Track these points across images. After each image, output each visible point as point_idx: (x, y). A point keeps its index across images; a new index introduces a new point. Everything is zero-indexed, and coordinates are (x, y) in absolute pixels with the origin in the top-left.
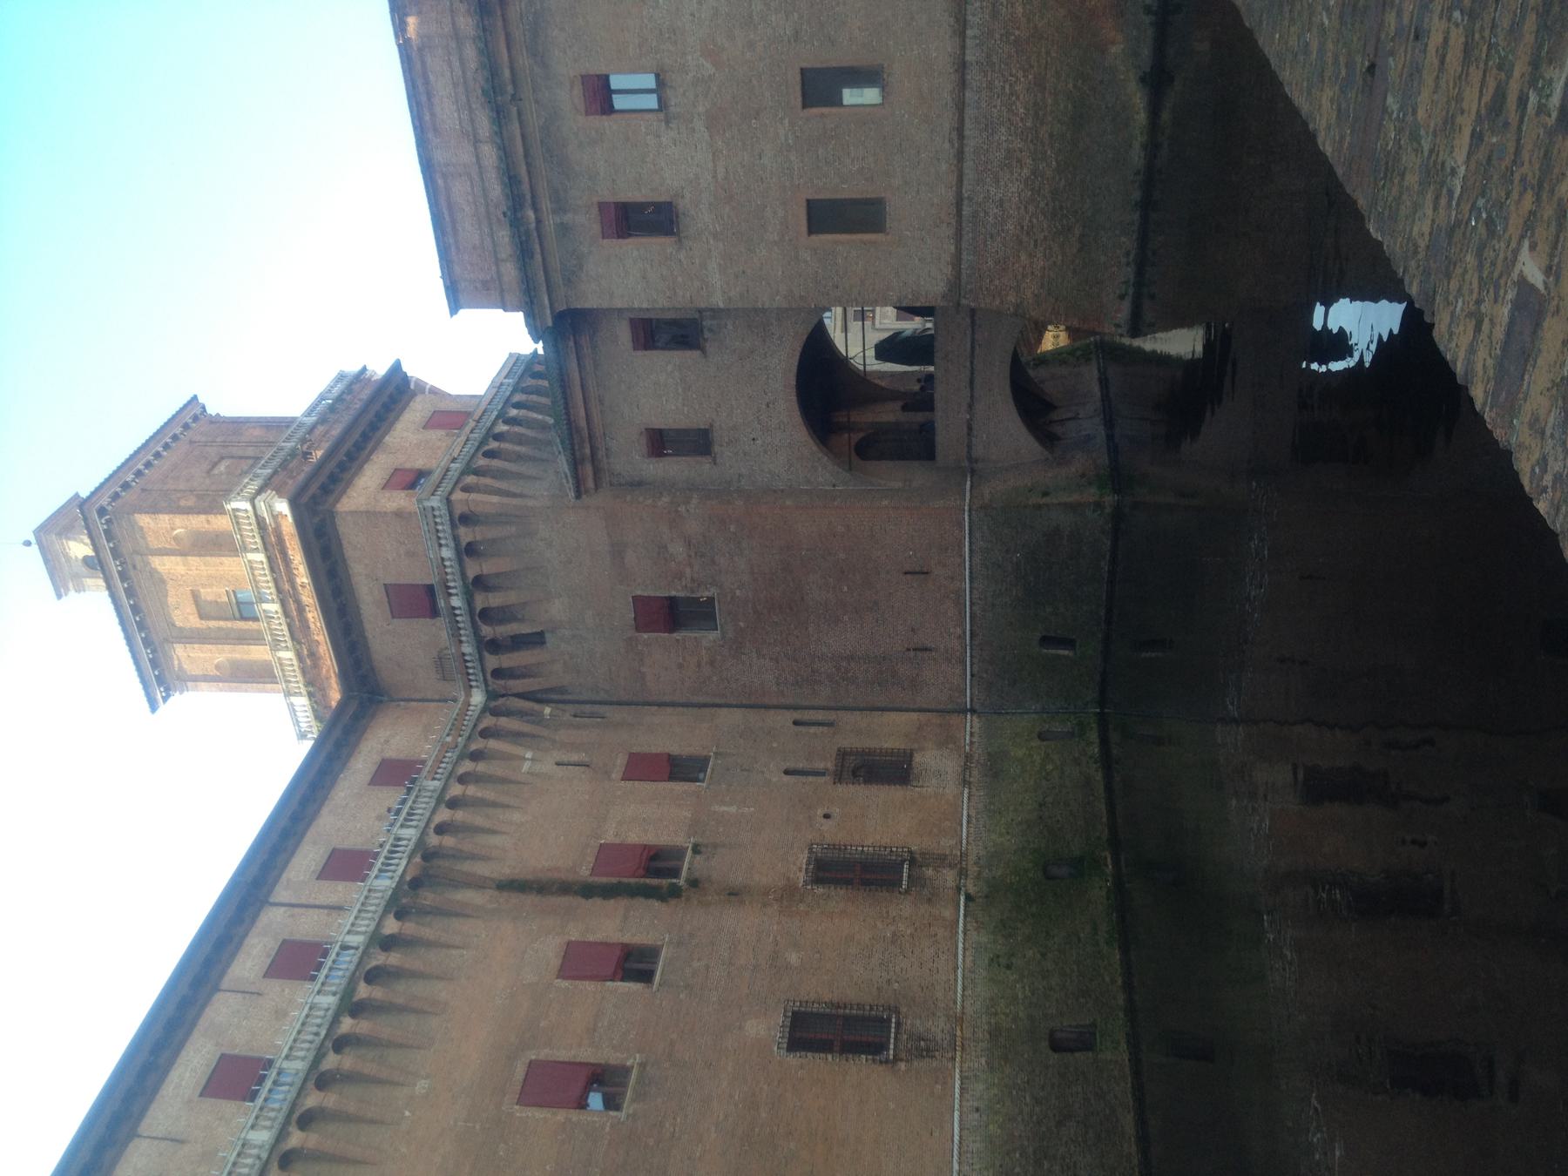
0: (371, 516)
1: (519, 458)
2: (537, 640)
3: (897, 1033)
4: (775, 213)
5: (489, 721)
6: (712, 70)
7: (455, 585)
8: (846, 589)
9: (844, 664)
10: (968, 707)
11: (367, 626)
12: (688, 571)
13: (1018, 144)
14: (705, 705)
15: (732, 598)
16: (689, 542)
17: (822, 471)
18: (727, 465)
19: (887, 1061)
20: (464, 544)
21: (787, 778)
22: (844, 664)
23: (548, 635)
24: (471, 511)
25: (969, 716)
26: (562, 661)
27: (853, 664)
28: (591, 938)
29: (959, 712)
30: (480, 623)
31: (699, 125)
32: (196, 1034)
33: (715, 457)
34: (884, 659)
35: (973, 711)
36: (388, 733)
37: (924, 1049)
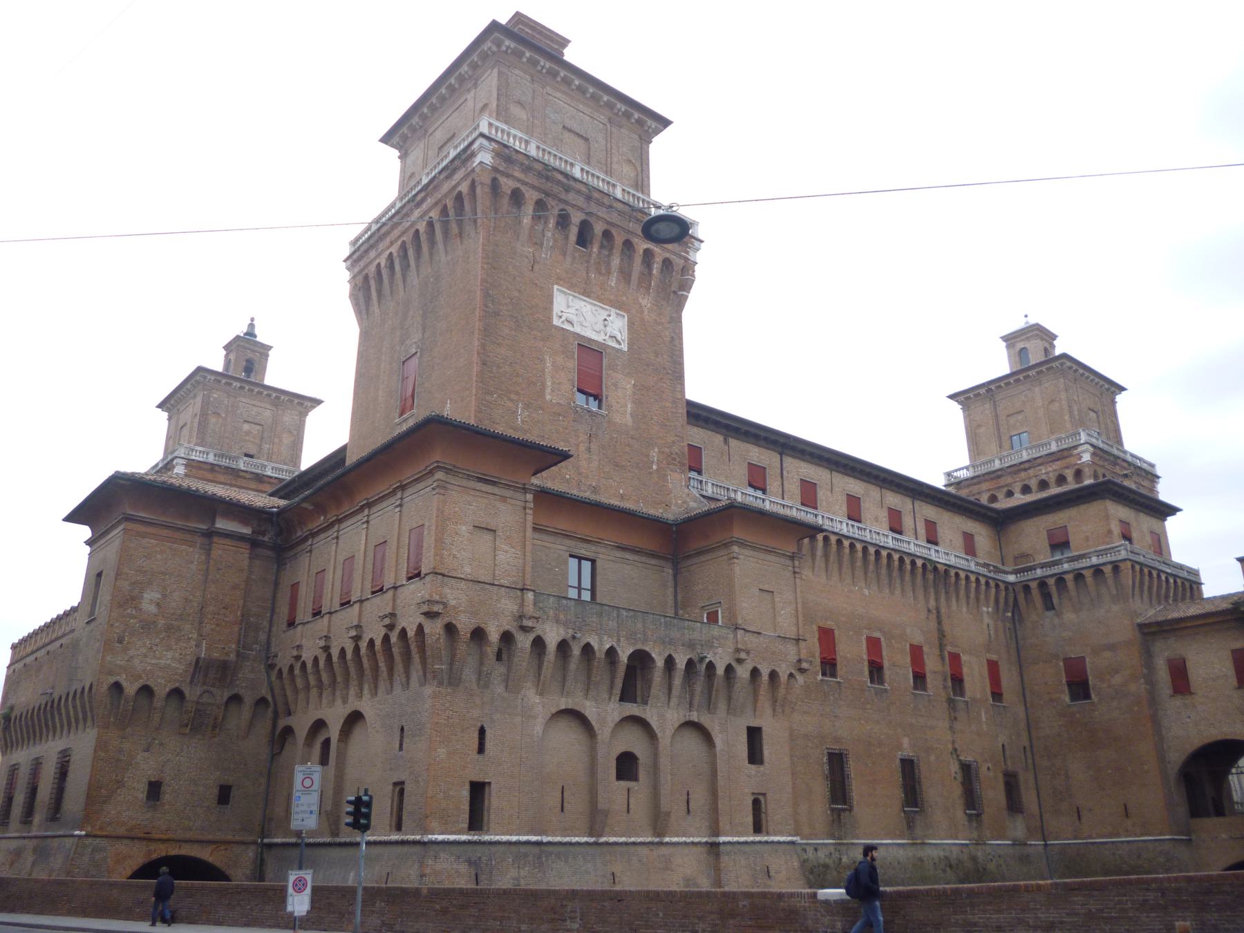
1: (1150, 588)
5: (1002, 586)
7: (1077, 565)
8: (1109, 771)
10: (1048, 842)
17: (1176, 758)
19: (903, 807)
20: (1102, 568)
21: (1000, 745)
23: (1053, 612)
25: (1043, 843)
28: (925, 657)
32: (865, 484)
35: (1046, 845)
36: (984, 534)
37: (910, 825)
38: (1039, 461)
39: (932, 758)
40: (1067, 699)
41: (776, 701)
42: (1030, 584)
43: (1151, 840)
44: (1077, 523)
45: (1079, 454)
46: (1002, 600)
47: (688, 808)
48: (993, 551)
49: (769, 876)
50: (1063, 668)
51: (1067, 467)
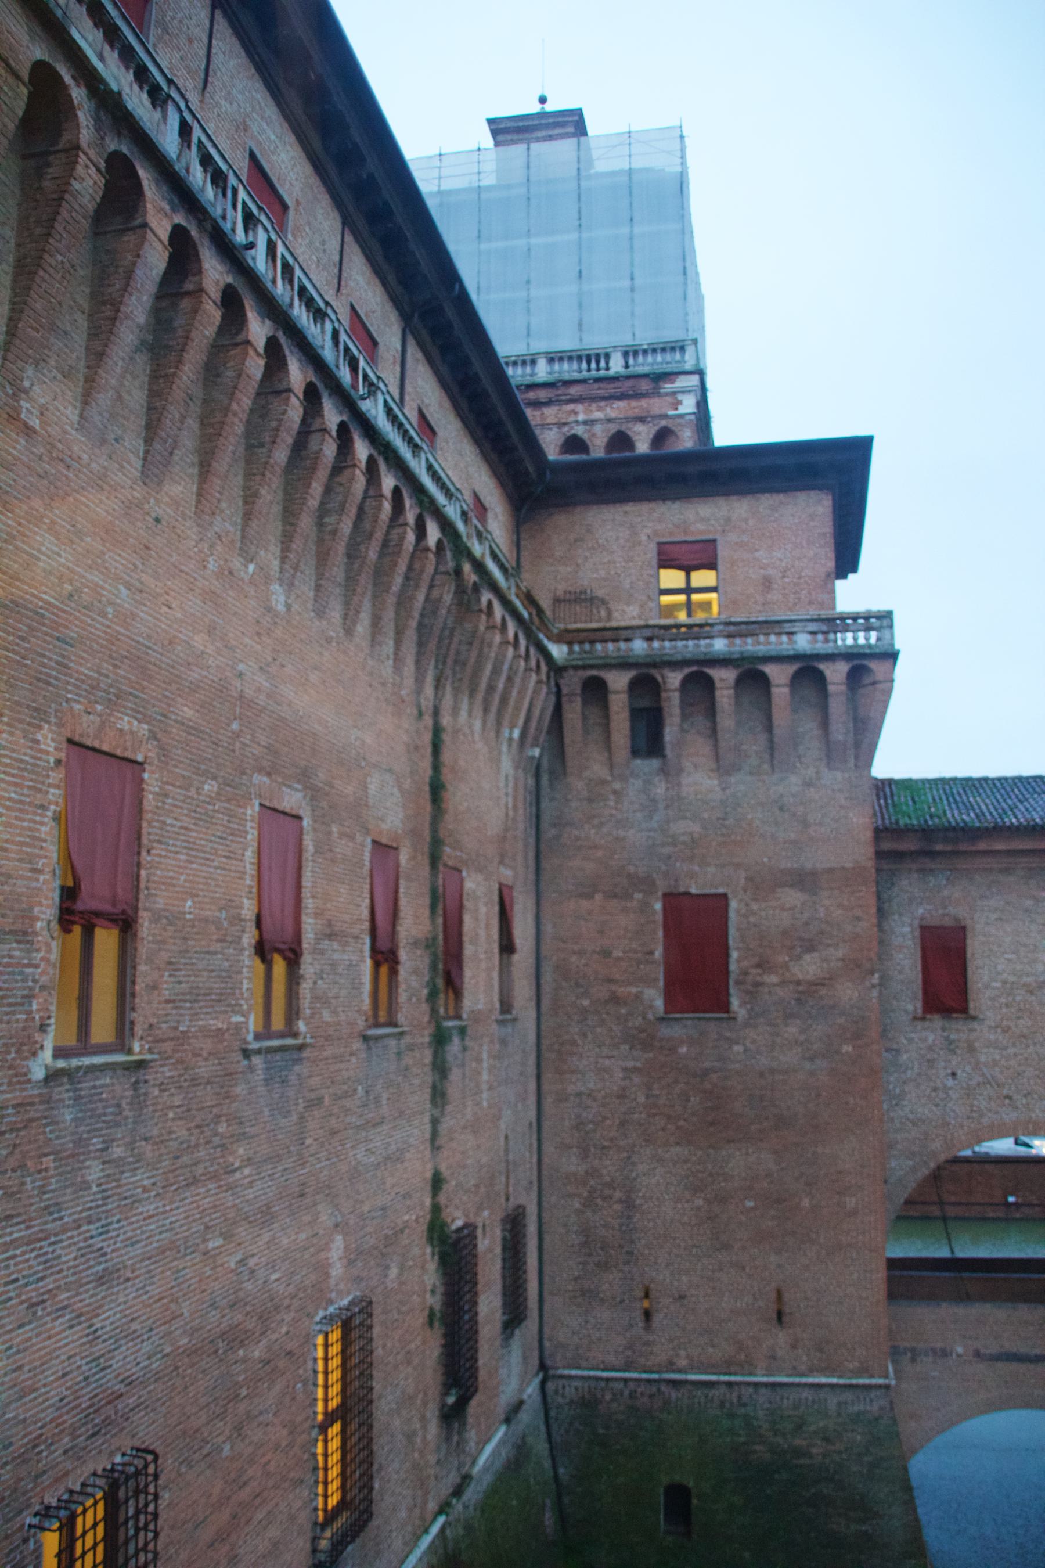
7: (750, 646)
8: (750, 1204)
11: (645, 507)
12: (774, 979)
15: (728, 1038)
16: (823, 985)
18: (913, 1035)
20: (822, 666)
22: (618, 1194)
23: (655, 763)
24: (874, 683)
26: (609, 778)
27: (617, 1207)
30: (687, 671)
33: (923, 1019)
34: (630, 1253)
38: (574, 390)
40: (659, 1003)
43: (832, 1386)
44: (745, 538)
45: (674, 394)
50: (659, 917)
51: (641, 420)
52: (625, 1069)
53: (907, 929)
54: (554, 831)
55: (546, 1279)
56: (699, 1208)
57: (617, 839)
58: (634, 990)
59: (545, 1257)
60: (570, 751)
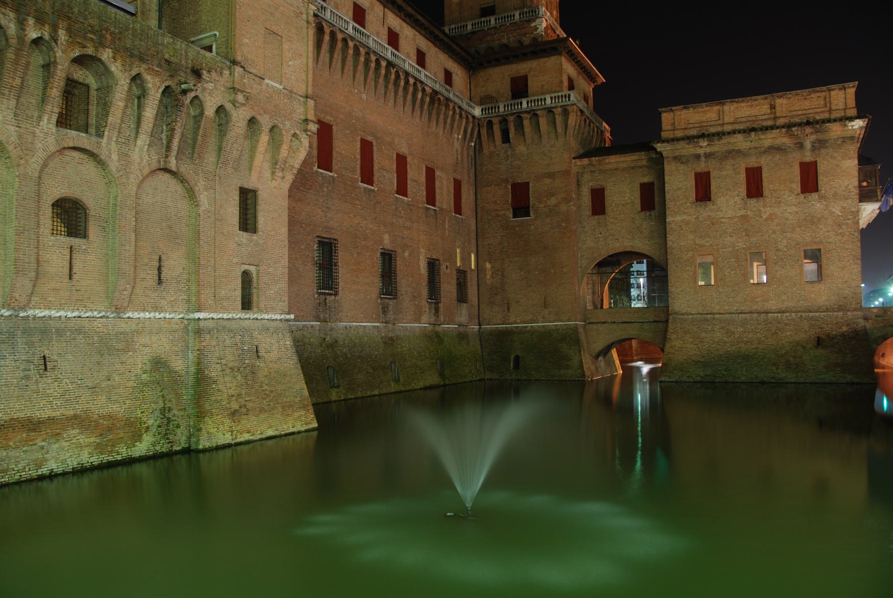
0: (561, 70)
2: (506, 139)
3: (388, 298)
4: (707, 242)
6: (764, 217)
8: (536, 273)
9: (500, 273)
11: (506, 67)
12: (543, 206)
13: (737, 336)
14: (476, 213)
22: (500, 273)
23: (508, 145)
28: (408, 167)
29: (479, 322)
31: (742, 212)
35: (480, 328)
37: (385, 310)
39: (406, 254)
40: (511, 215)
41: (276, 164)
42: (493, 119)
46: (469, 131)
47: (160, 277)
48: (465, 91)
49: (258, 357)
50: (510, 190)
52: (501, 236)
53: (587, 190)
54: (480, 168)
55: (480, 300)
56: (522, 275)
57: (498, 168)
58: (503, 212)
59: (480, 293)
60: (484, 143)
